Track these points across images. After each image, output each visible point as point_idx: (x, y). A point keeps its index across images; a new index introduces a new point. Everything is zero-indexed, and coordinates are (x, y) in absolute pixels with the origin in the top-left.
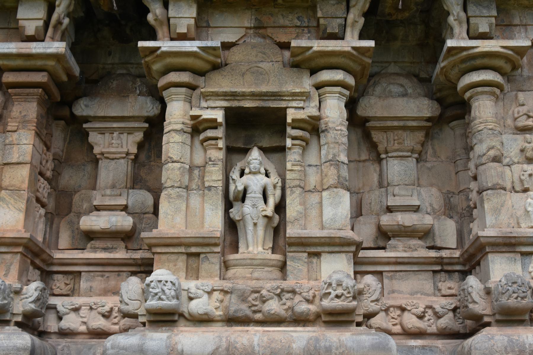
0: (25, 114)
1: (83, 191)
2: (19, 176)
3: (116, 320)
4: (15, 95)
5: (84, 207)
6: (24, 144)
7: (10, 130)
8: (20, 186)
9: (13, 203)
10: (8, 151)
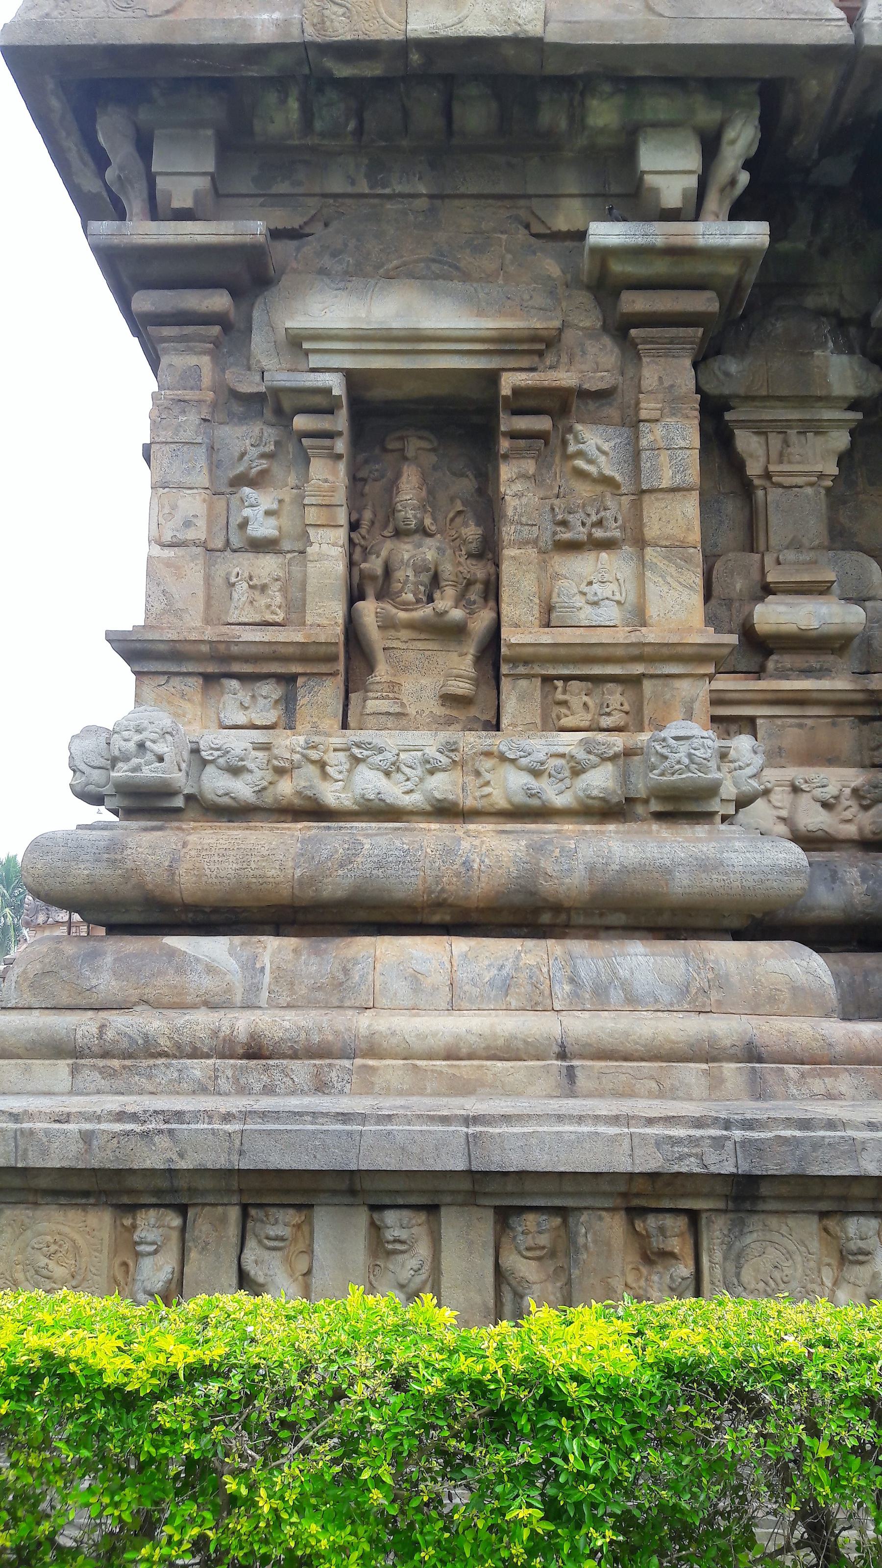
1: (731, 555)
3: (848, 814)
4: (645, 341)
5: (738, 586)
6: (680, 448)
9: (674, 573)
10: (649, 464)
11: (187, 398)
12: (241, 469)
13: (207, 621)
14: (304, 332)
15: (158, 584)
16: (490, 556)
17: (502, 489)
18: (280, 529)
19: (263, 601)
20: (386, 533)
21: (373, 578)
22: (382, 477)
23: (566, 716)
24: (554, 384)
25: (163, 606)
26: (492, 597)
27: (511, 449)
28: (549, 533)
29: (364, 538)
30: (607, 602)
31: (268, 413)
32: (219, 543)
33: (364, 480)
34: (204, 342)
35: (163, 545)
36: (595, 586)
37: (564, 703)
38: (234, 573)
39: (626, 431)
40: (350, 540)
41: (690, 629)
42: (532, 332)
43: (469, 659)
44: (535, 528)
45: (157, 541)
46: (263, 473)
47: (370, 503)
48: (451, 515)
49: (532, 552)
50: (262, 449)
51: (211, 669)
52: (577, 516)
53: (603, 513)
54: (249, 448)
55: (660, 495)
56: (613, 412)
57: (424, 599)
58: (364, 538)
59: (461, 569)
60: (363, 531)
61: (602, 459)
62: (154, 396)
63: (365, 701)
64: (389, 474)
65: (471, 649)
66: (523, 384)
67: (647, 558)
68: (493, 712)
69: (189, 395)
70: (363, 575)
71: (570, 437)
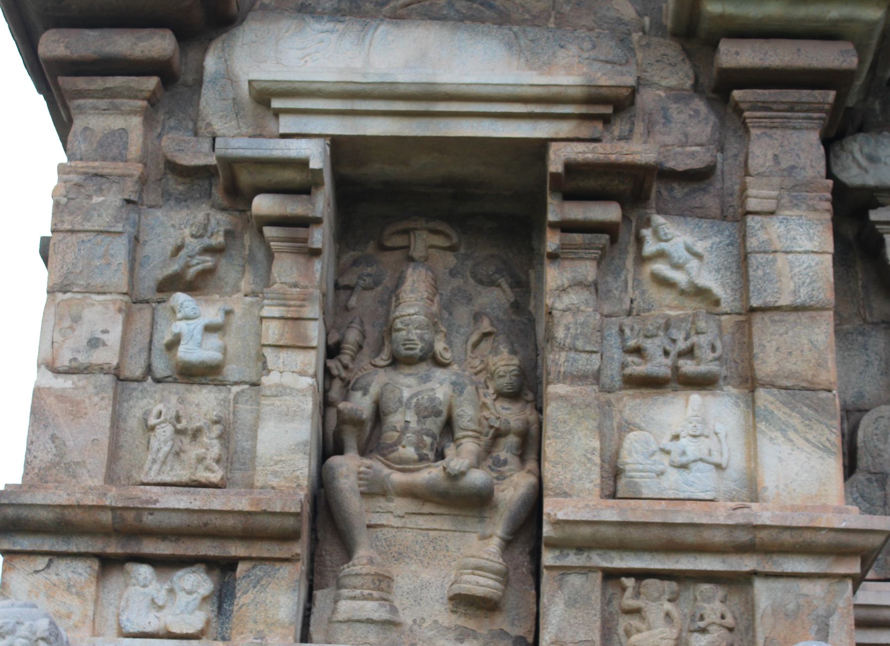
0: (792, 163)
2: (806, 347)
4: (755, 107)
6: (806, 252)
7: (758, 208)
8: (813, 375)
11: (105, 171)
12: (174, 267)
13: (111, 478)
14: (274, 87)
15: (46, 426)
16: (530, 397)
17: (549, 301)
18: (224, 351)
19: (193, 451)
20: (379, 362)
21: (358, 423)
22: (377, 283)
23: (639, 631)
24: (624, 159)
25: (50, 456)
26: (532, 456)
27: (563, 246)
28: (616, 366)
29: (346, 367)
30: (701, 465)
31: (218, 194)
32: (136, 368)
33: (350, 288)
34: (136, 98)
35: (57, 372)
36: (683, 441)
37: (636, 612)
38: (155, 412)
39: (729, 228)
40: (327, 371)
41: (825, 508)
42: (593, 90)
43: (494, 545)
44: (596, 358)
45: (49, 365)
46: (207, 273)
47: (357, 320)
48: (474, 338)
49: (590, 390)
50: (206, 241)
51: (113, 548)
52: (657, 341)
53: (694, 339)
54: (189, 240)
55: (777, 316)
56: (710, 202)
57: (431, 455)
58: (346, 367)
59: (486, 413)
60: (346, 358)
61: (694, 263)
62: (62, 169)
63: (336, 602)
64: (388, 281)
65: (498, 527)
66: (580, 158)
67: (760, 403)
68: (531, 624)
69: (107, 167)
70: (343, 420)
71: (647, 233)
